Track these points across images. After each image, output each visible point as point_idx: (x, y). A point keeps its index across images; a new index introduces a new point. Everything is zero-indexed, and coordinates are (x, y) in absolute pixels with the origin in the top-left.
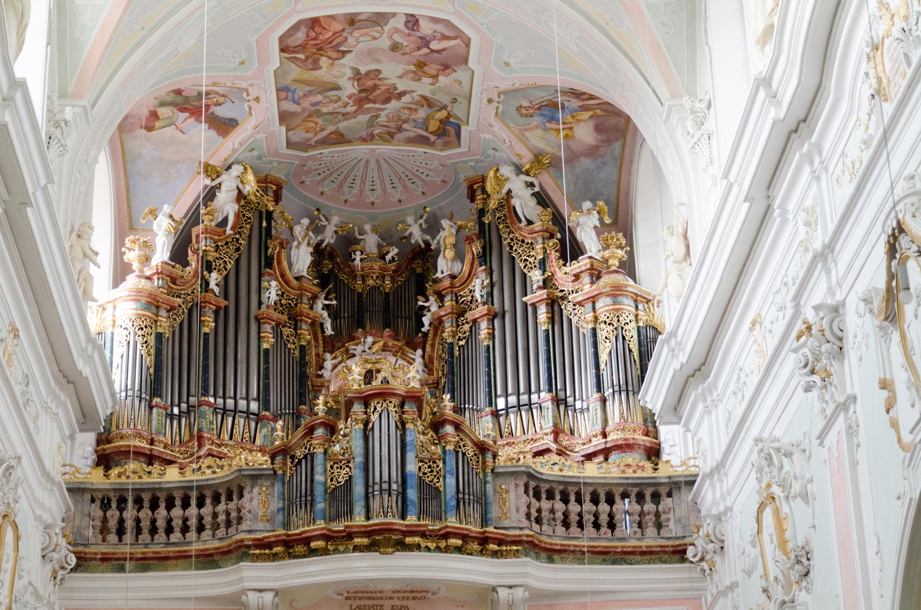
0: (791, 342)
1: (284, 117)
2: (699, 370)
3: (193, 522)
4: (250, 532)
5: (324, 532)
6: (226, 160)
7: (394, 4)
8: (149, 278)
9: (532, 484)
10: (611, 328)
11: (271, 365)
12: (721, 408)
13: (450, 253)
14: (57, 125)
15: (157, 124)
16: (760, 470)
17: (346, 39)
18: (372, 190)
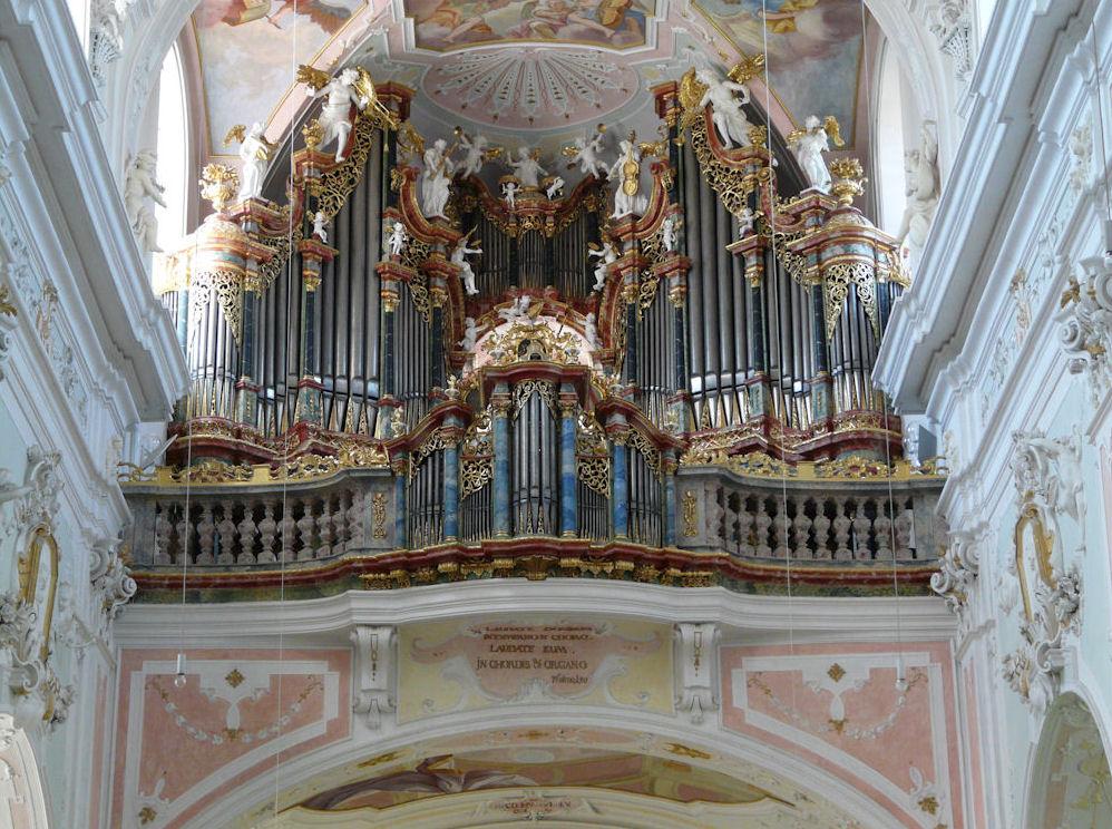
0: (1056, 310)
2: (947, 343)
3: (287, 538)
5: (455, 551)
6: (335, 63)
8: (236, 220)
9: (728, 491)
10: (843, 286)
11: (396, 334)
12: (977, 390)
13: (632, 186)
14: (106, 23)
15: (244, 16)
16: (1020, 474)
18: (531, 102)
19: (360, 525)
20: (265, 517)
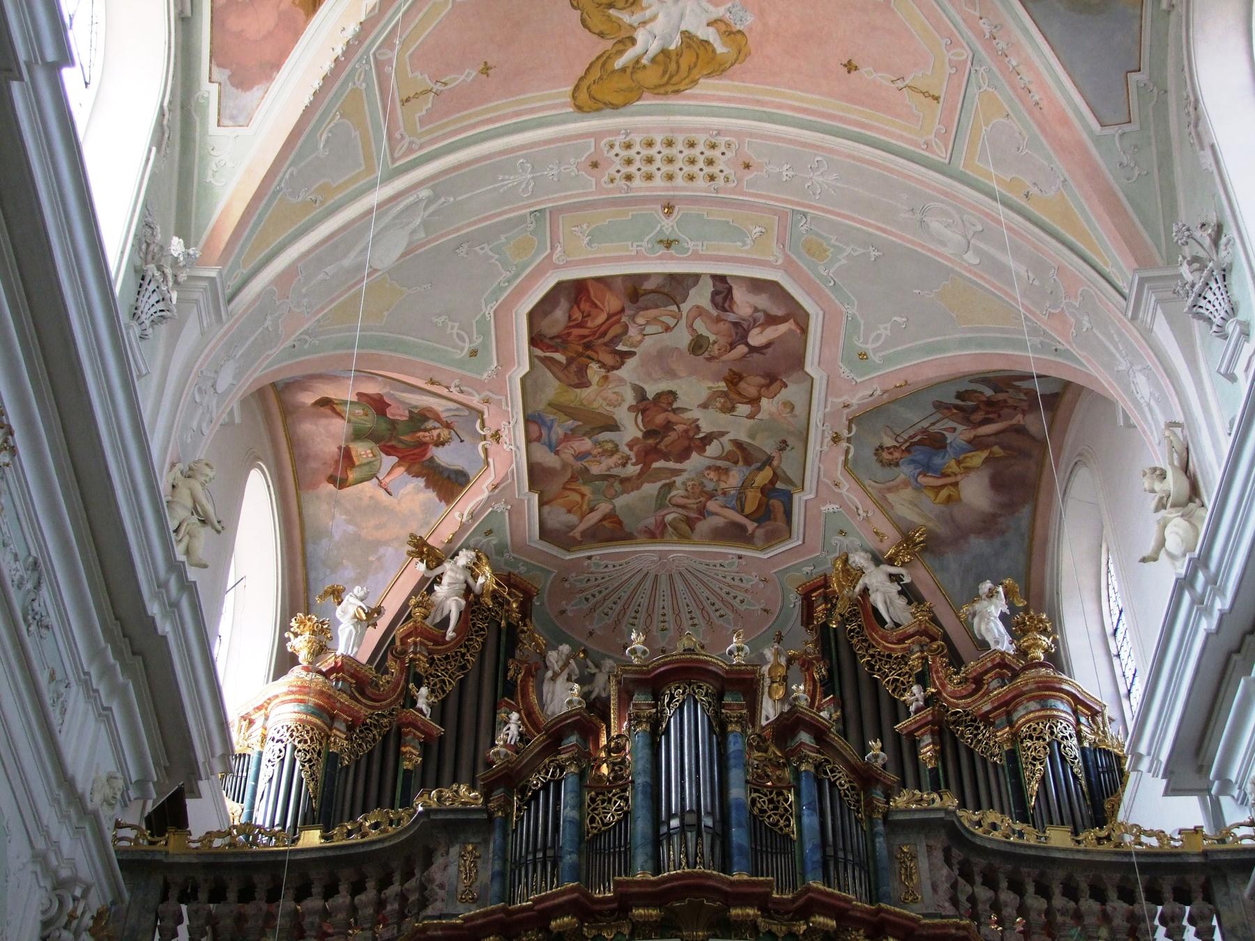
1: (537, 475)
4: (440, 917)
6: (450, 541)
7: (697, 257)
15: (352, 475)
17: (626, 328)
19: (442, 886)
20: (310, 895)
